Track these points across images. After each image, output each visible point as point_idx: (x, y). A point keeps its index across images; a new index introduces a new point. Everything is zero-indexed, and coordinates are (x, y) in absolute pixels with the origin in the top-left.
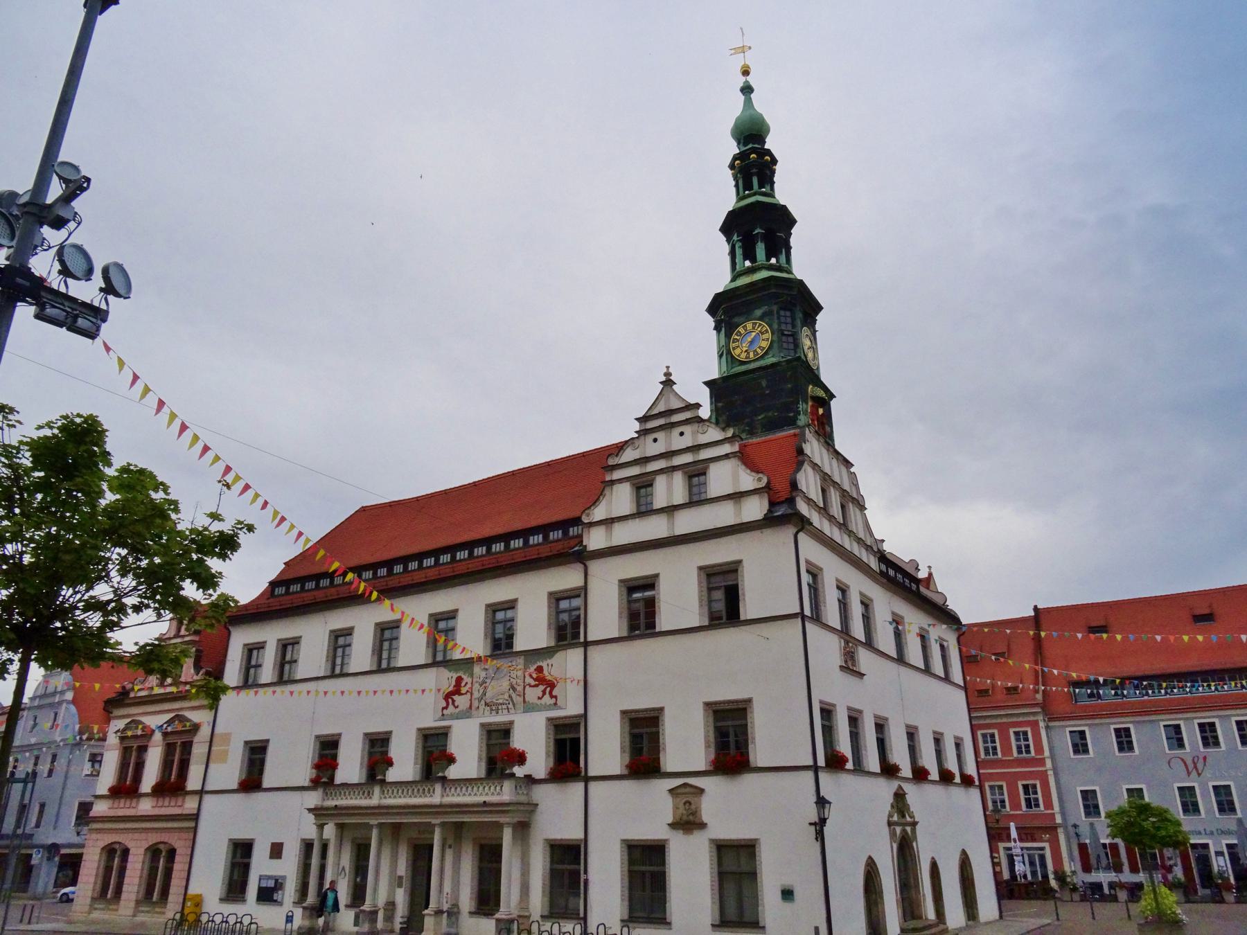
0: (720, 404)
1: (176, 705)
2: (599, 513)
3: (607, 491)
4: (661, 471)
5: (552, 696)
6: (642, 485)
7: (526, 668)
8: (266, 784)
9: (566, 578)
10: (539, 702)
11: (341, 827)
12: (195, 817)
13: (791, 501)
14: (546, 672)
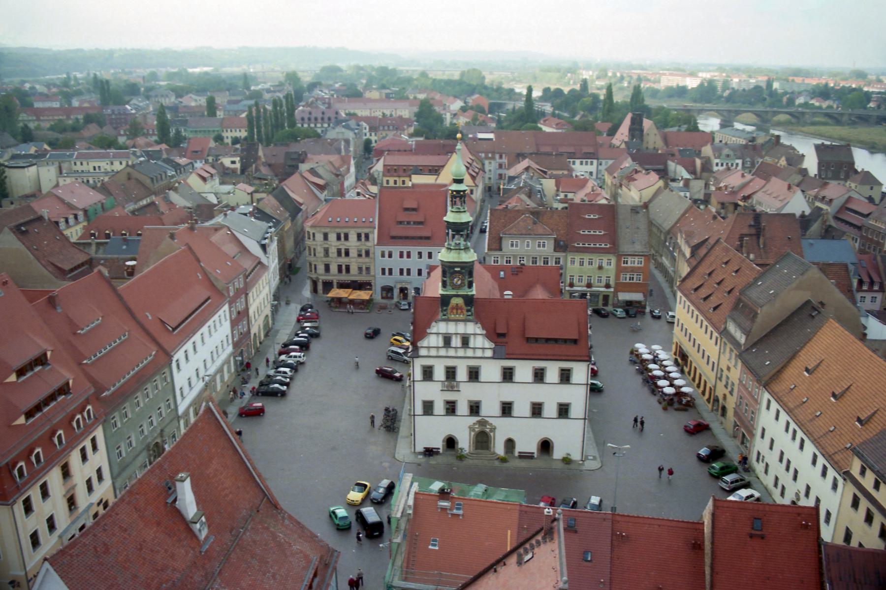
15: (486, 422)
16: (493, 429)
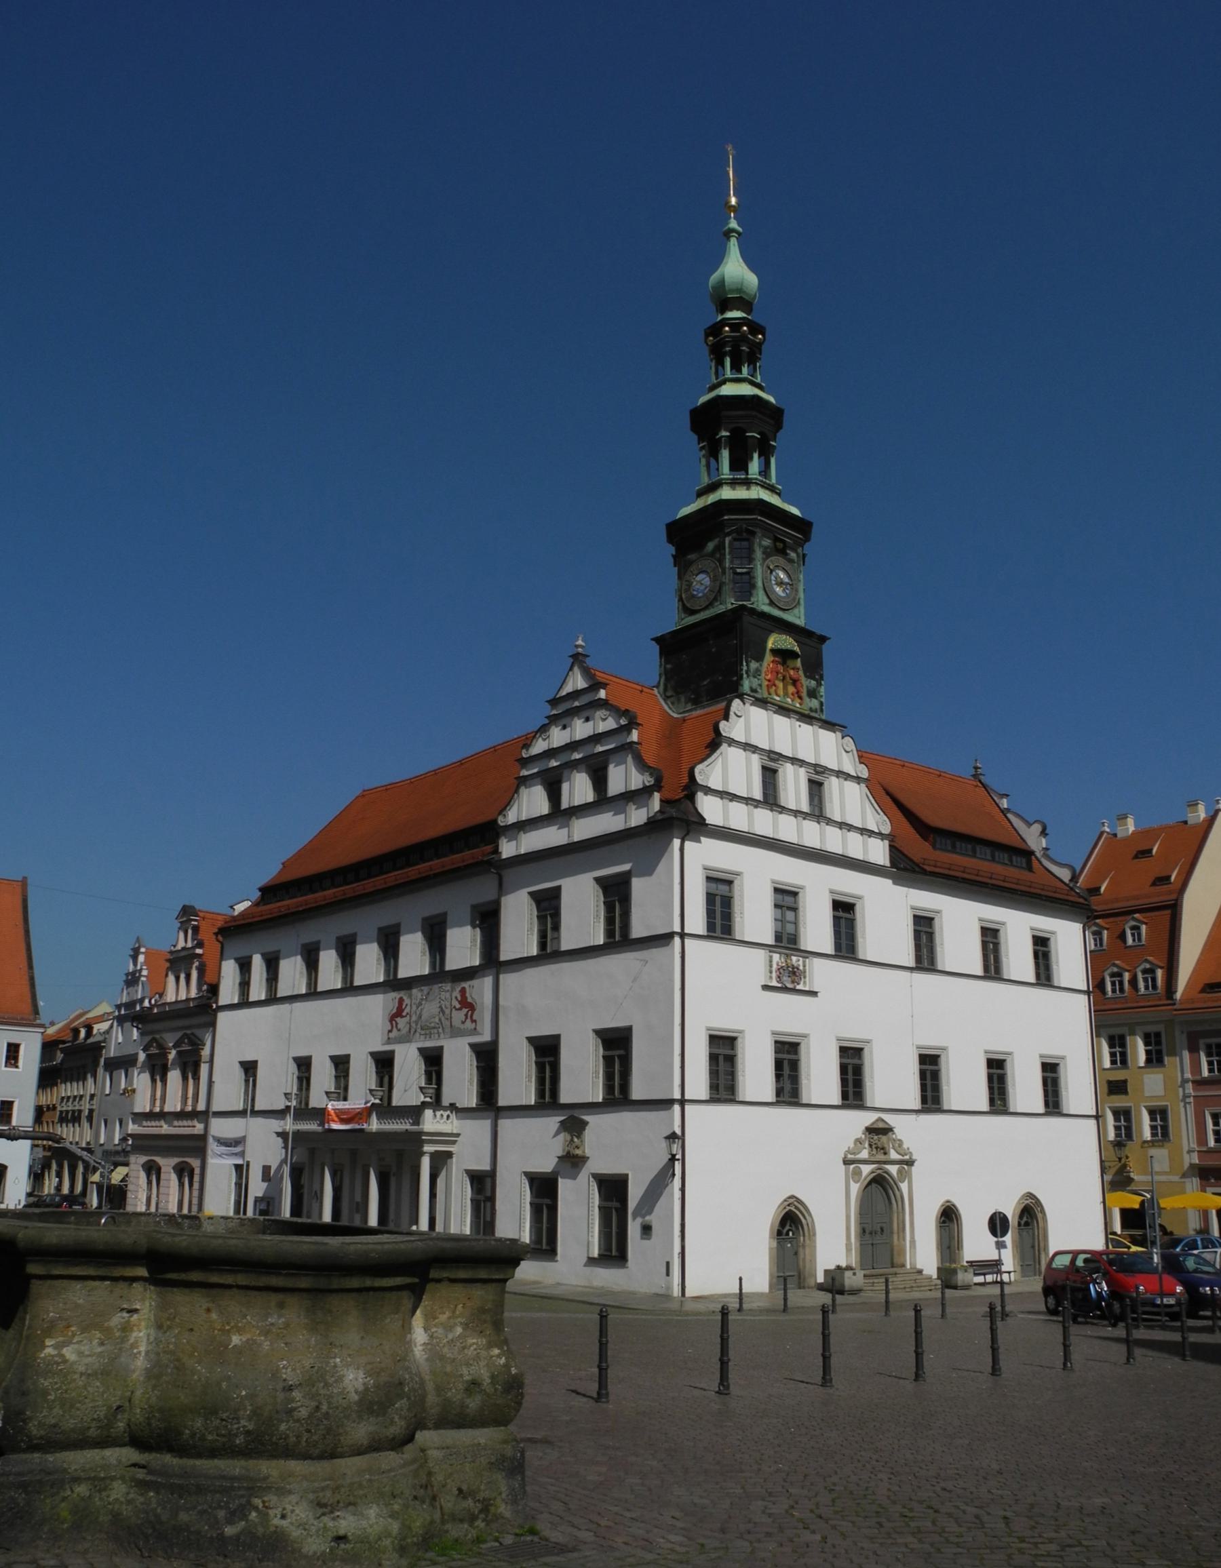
0: (669, 666)
1: (186, 1022)
2: (512, 817)
5: (474, 1021)
7: (453, 990)
10: (462, 1027)
14: (468, 995)
15: (887, 1131)
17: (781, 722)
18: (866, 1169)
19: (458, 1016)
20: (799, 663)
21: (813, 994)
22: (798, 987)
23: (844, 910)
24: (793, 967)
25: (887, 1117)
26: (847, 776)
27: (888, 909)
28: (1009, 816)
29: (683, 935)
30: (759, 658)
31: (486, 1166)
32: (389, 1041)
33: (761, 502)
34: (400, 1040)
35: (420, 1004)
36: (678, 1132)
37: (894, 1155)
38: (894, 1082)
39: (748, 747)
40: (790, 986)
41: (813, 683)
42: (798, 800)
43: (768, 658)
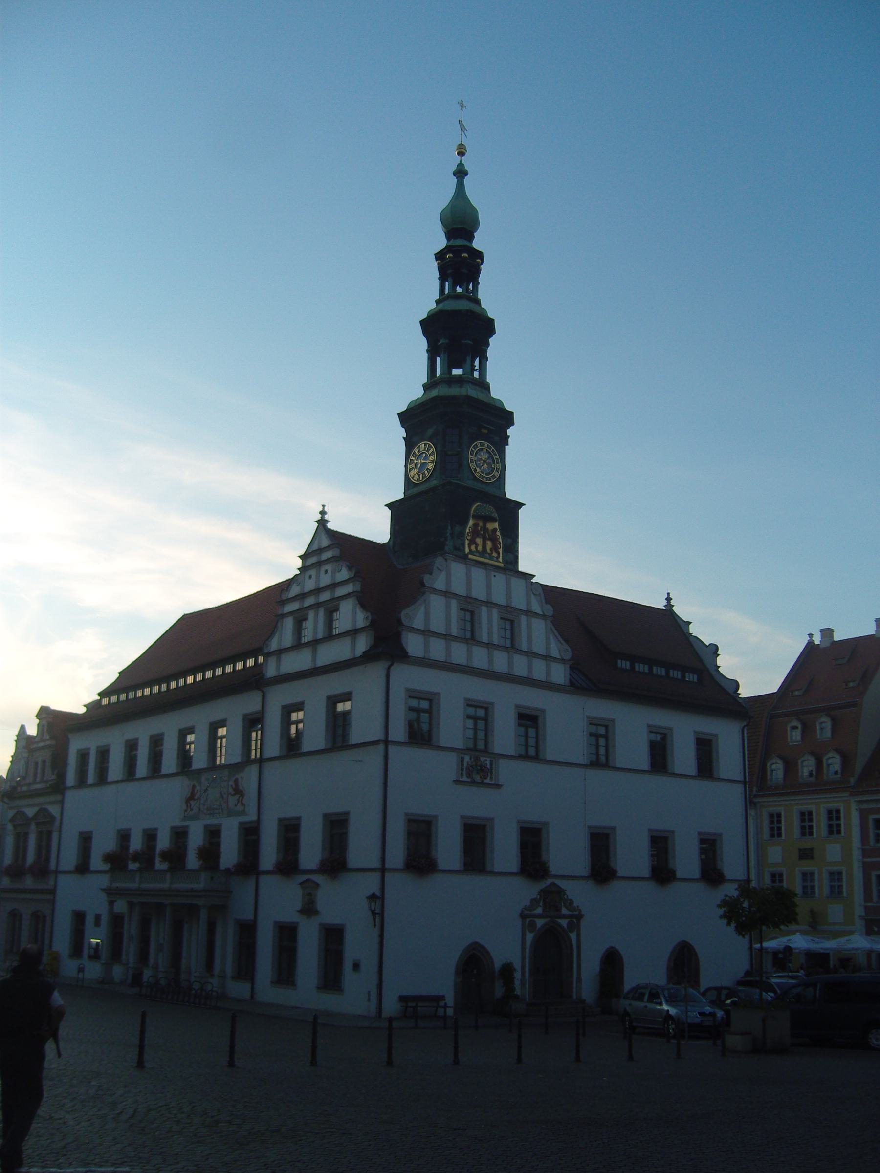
3: (279, 624)
4: (310, 607)
5: (243, 804)
6: (300, 619)
8: (92, 868)
9: (250, 703)
11: (131, 905)
12: (53, 892)
13: (398, 636)
15: (560, 892)
16: (577, 918)
17: (478, 574)
18: (540, 922)
19: (232, 800)
20: (496, 525)
21: (498, 786)
22: (487, 781)
23: (529, 720)
24: (481, 766)
25: (558, 882)
26: (535, 615)
27: (567, 720)
28: (691, 639)
29: (386, 742)
30: (466, 523)
31: (250, 916)
32: (185, 818)
33: (468, 398)
34: (192, 818)
35: (206, 791)
36: (378, 894)
37: (564, 911)
38: (567, 854)
39: (447, 594)
40: (477, 778)
41: (510, 541)
42: (490, 633)
43: (471, 522)
